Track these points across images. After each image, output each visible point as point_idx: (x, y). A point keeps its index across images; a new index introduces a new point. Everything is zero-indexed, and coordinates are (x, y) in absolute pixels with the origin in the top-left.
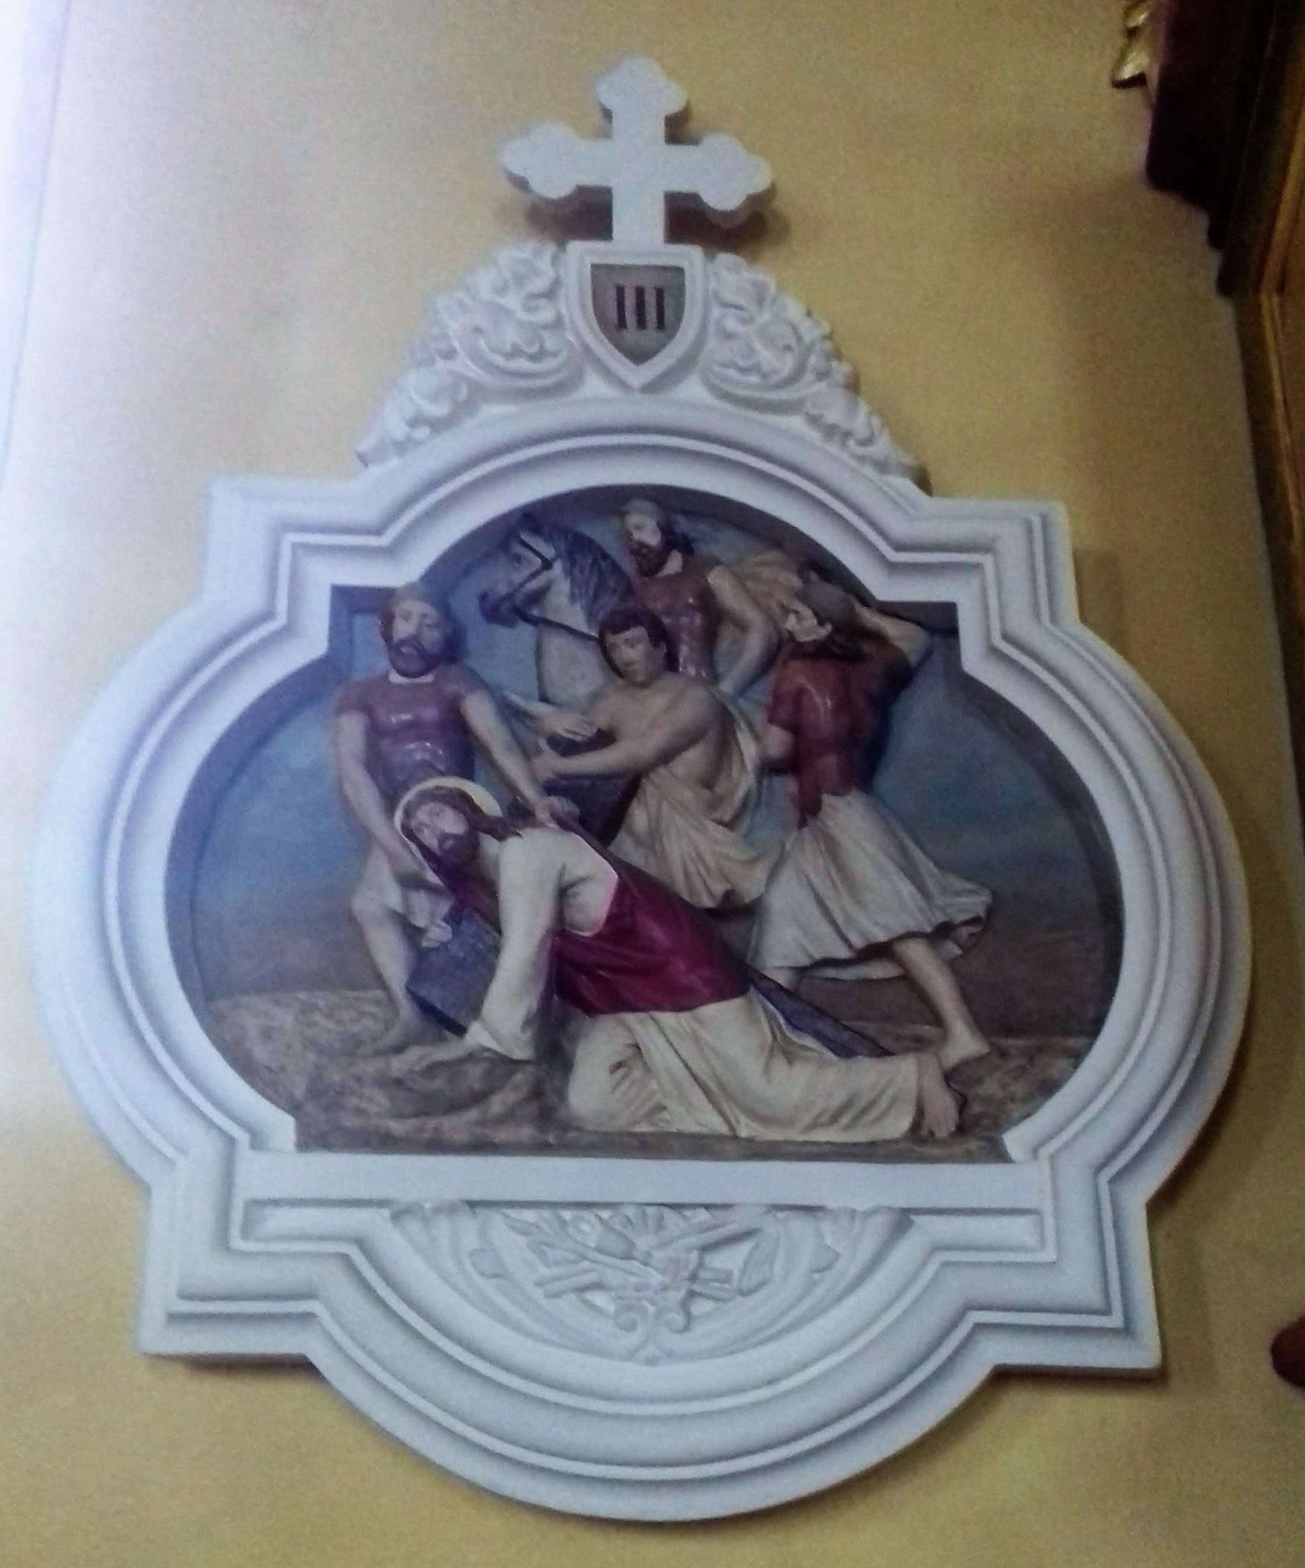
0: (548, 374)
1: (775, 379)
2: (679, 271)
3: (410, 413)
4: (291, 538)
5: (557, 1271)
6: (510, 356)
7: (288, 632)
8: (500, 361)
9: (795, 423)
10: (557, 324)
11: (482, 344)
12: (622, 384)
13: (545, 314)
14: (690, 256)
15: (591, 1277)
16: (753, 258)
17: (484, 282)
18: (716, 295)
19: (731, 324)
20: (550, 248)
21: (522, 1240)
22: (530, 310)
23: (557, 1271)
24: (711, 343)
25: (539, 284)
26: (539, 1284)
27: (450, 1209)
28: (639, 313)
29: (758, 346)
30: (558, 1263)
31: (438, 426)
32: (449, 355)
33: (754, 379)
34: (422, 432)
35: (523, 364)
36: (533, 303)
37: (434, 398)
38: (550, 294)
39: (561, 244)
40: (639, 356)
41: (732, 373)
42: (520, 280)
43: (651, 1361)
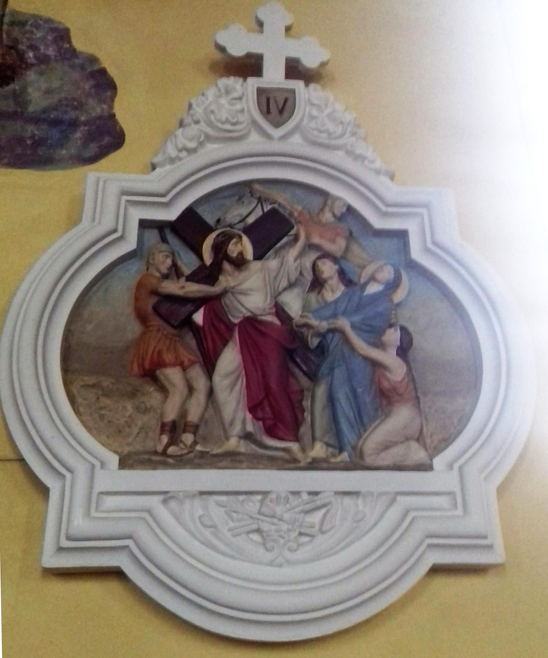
0: (240, 131)
1: (333, 135)
2: (293, 91)
3: (180, 146)
4: (125, 198)
5: (237, 524)
6: (223, 123)
7: (121, 238)
8: (220, 125)
9: (341, 153)
10: (242, 111)
11: (212, 117)
12: (269, 137)
13: (238, 107)
14: (298, 85)
15: (255, 527)
16: (324, 87)
17: (211, 93)
18: (309, 100)
19: (315, 112)
20: (241, 80)
21: (223, 510)
22: (232, 104)
23: (237, 524)
24: (306, 121)
25: (235, 95)
26: (229, 530)
27: (191, 496)
28: (276, 107)
29: (326, 120)
30: (239, 520)
31: (191, 151)
32: (197, 122)
33: (324, 135)
34: (184, 154)
35: (228, 127)
36: (234, 101)
37: (191, 140)
38: (240, 99)
39: (245, 79)
40: (277, 125)
41: (315, 133)
42: (227, 92)
43: (281, 566)
